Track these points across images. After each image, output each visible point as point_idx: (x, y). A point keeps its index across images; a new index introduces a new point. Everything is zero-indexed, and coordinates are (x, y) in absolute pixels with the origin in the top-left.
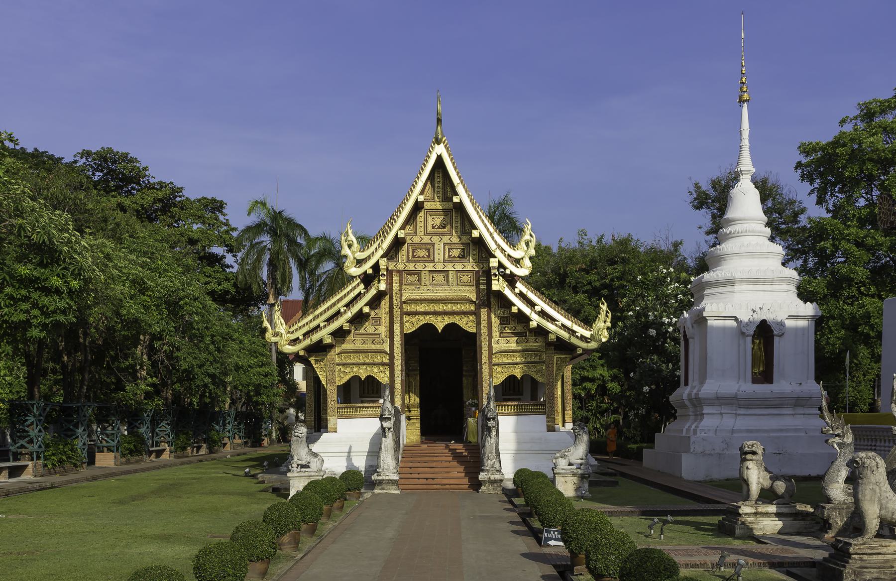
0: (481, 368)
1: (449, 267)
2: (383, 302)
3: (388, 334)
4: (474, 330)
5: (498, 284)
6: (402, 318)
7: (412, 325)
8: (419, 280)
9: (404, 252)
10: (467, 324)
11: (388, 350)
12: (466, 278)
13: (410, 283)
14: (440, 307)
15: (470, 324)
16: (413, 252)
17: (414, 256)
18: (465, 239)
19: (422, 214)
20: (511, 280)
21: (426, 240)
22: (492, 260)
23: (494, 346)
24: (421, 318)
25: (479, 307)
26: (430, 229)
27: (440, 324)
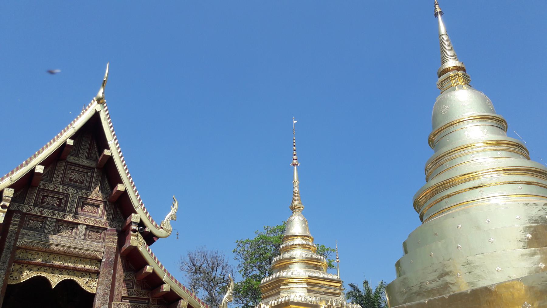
4: (93, 291)
5: (135, 240)
6: (10, 265)
15: (89, 284)
16: (43, 199)
21: (61, 189)
22: (133, 214)
26: (67, 180)
27: (55, 280)
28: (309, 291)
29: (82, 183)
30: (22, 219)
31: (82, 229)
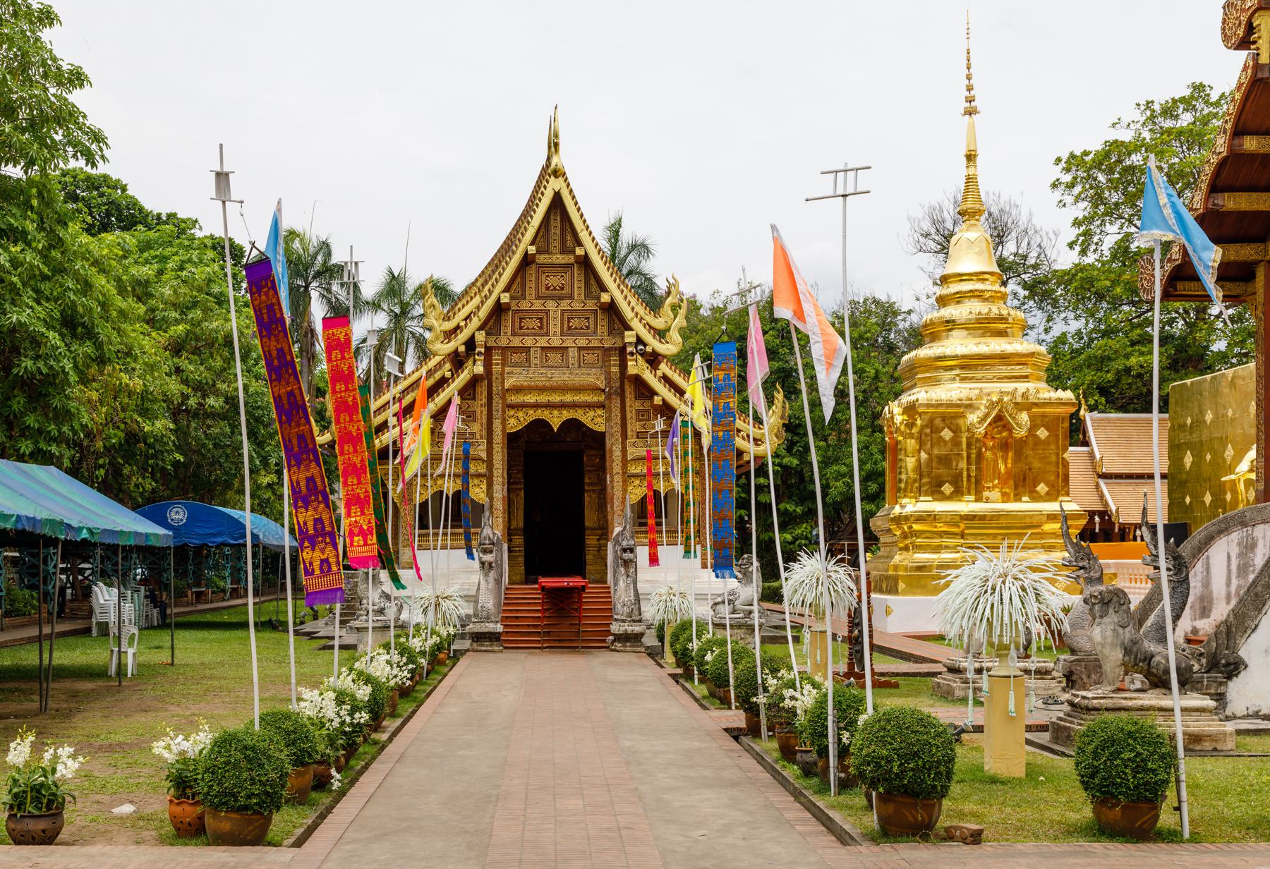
0: (612, 481)
1: (569, 342)
2: (478, 390)
3: (484, 433)
4: (602, 429)
5: (636, 366)
6: (504, 412)
7: (516, 422)
8: (528, 360)
9: (507, 323)
10: (594, 421)
11: (484, 455)
12: (590, 358)
13: (516, 365)
14: (556, 398)
15: (596, 420)
17: (521, 328)
18: (591, 304)
19: (532, 271)
20: (654, 360)
21: (538, 305)
22: (627, 333)
23: (630, 450)
24: (531, 412)
25: (609, 397)
26: (543, 290)
27: (556, 420)
29: (562, 289)
30: (503, 355)
31: (573, 353)
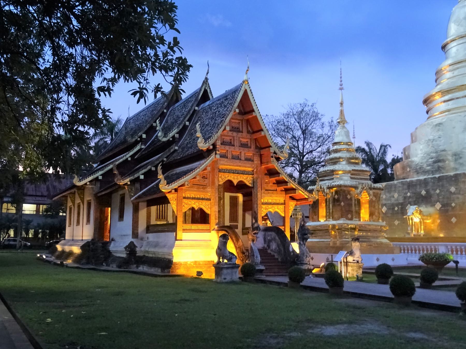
28: (351, 178)
